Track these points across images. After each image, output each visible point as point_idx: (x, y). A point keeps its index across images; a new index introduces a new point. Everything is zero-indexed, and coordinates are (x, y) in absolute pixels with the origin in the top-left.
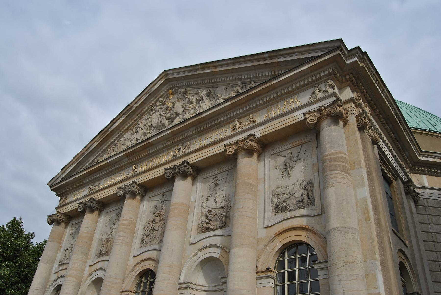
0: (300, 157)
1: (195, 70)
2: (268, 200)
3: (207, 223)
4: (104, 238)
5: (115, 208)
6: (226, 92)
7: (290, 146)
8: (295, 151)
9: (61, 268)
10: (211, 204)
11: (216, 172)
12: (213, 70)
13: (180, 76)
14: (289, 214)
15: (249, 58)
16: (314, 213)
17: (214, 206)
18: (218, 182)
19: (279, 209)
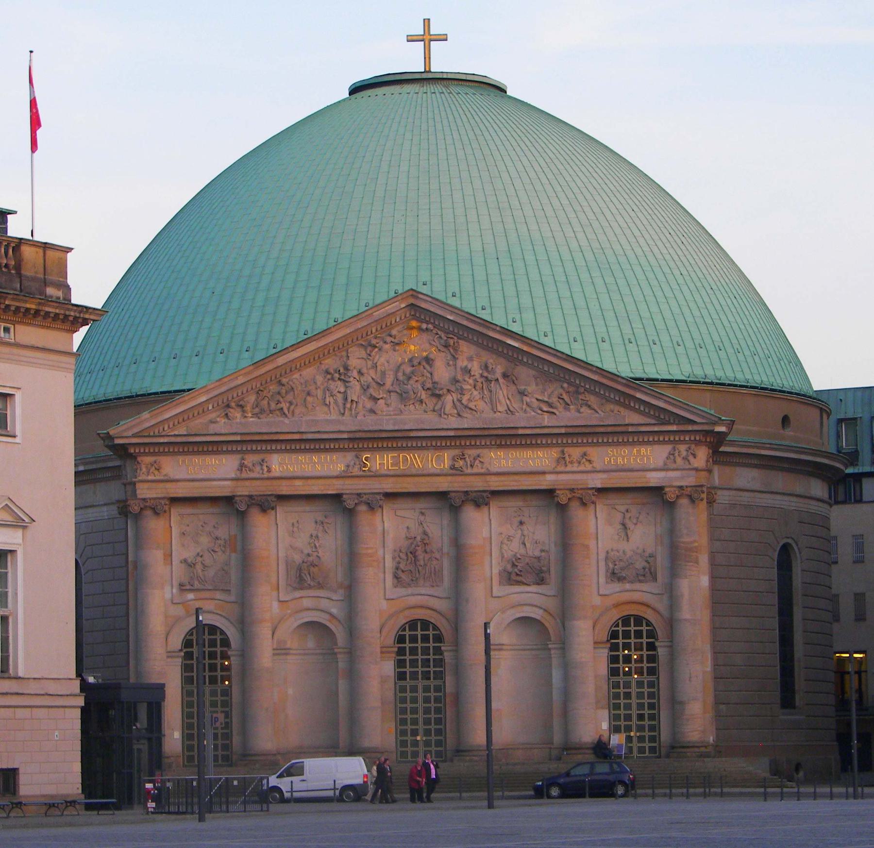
0: (641, 518)
1: (488, 328)
2: (602, 564)
3: (517, 575)
4: (297, 558)
5: (308, 508)
6: (537, 385)
7: (628, 501)
8: (634, 510)
9: (191, 596)
10: (514, 548)
11: (520, 503)
12: (525, 348)
13: (449, 317)
14: (628, 586)
15: (594, 369)
16: (657, 592)
17: (523, 551)
18: (524, 519)
19: (614, 576)
